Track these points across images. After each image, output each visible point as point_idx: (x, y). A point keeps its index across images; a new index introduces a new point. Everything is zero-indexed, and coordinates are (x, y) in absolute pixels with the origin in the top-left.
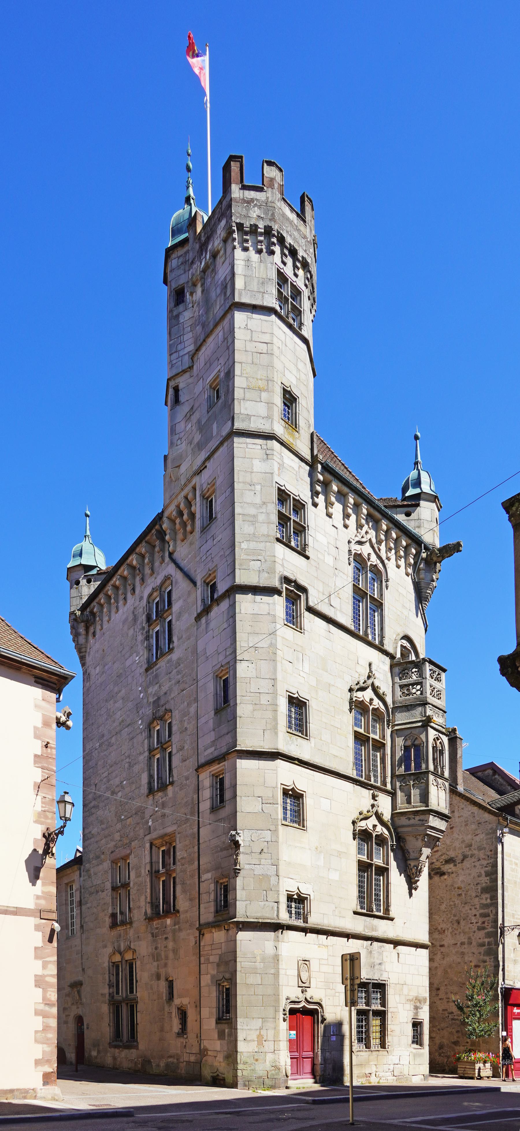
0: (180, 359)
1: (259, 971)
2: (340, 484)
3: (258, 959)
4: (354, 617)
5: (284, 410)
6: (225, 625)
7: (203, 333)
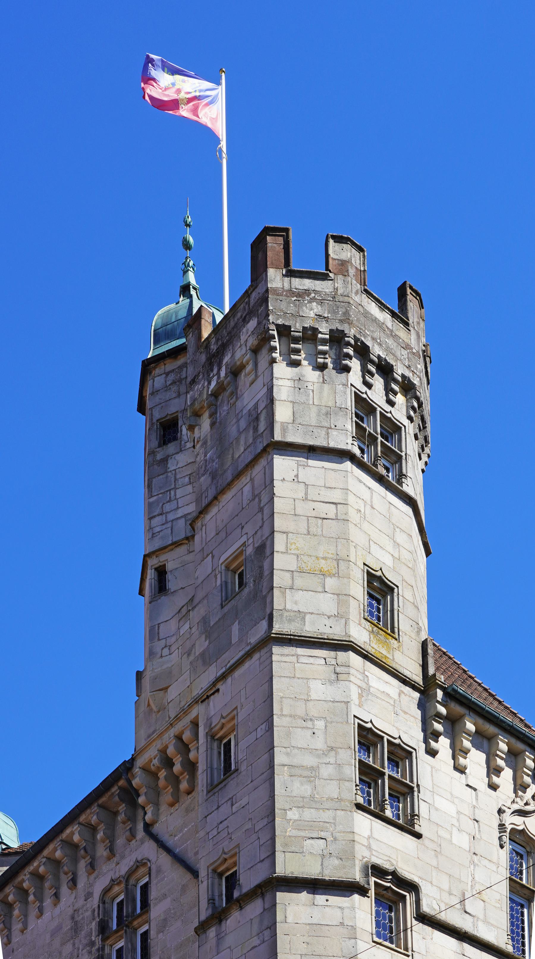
0: (169, 525)
2: (480, 721)
4: (512, 931)
5: (370, 605)
6: (256, 941)
7: (213, 487)
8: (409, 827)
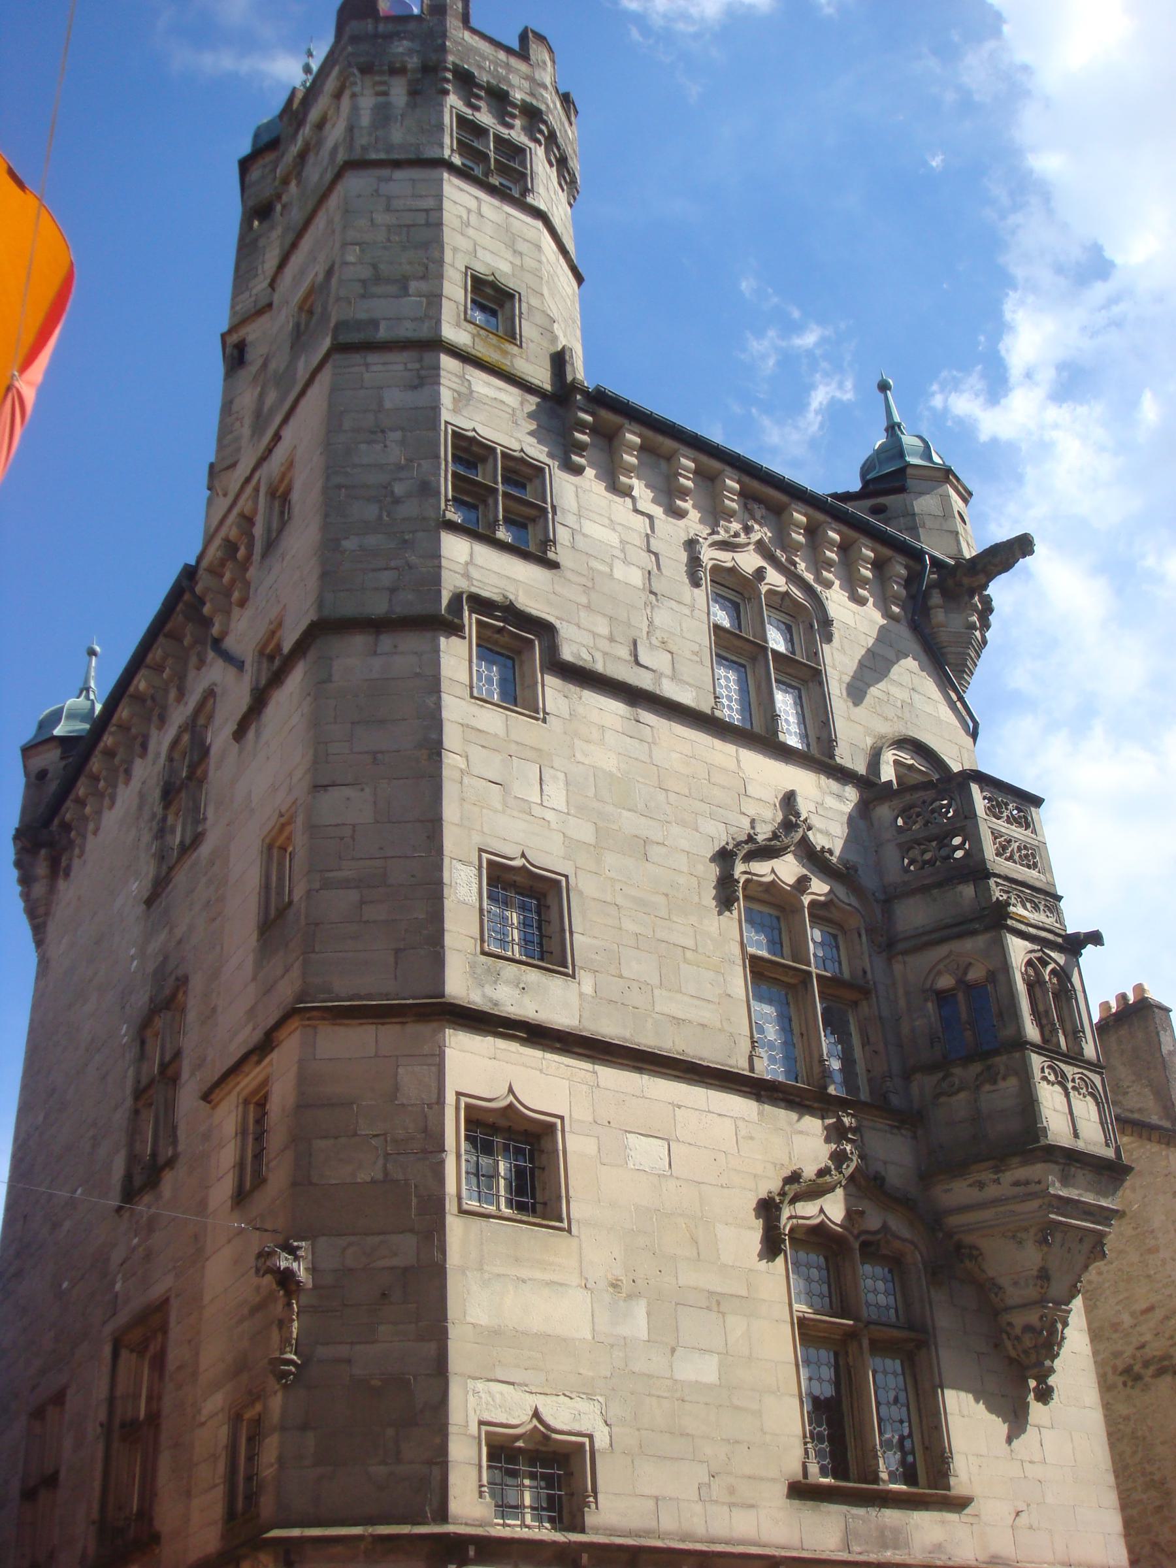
8: (540, 553)
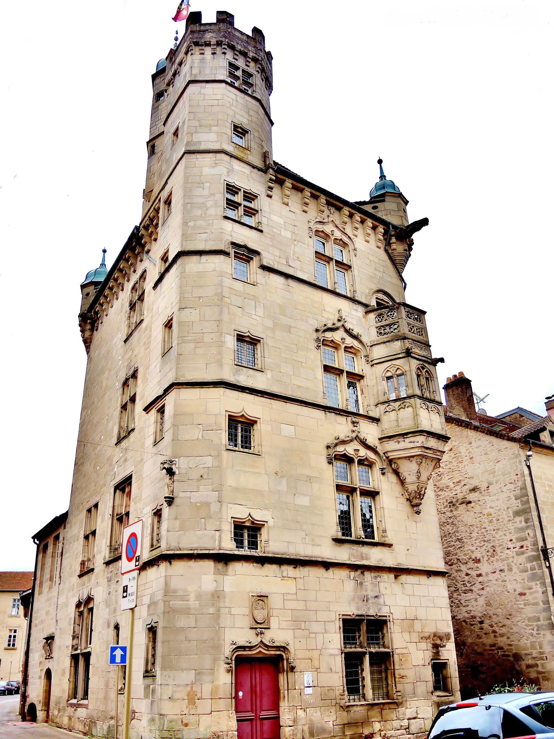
1: (193, 612)
3: (192, 597)
